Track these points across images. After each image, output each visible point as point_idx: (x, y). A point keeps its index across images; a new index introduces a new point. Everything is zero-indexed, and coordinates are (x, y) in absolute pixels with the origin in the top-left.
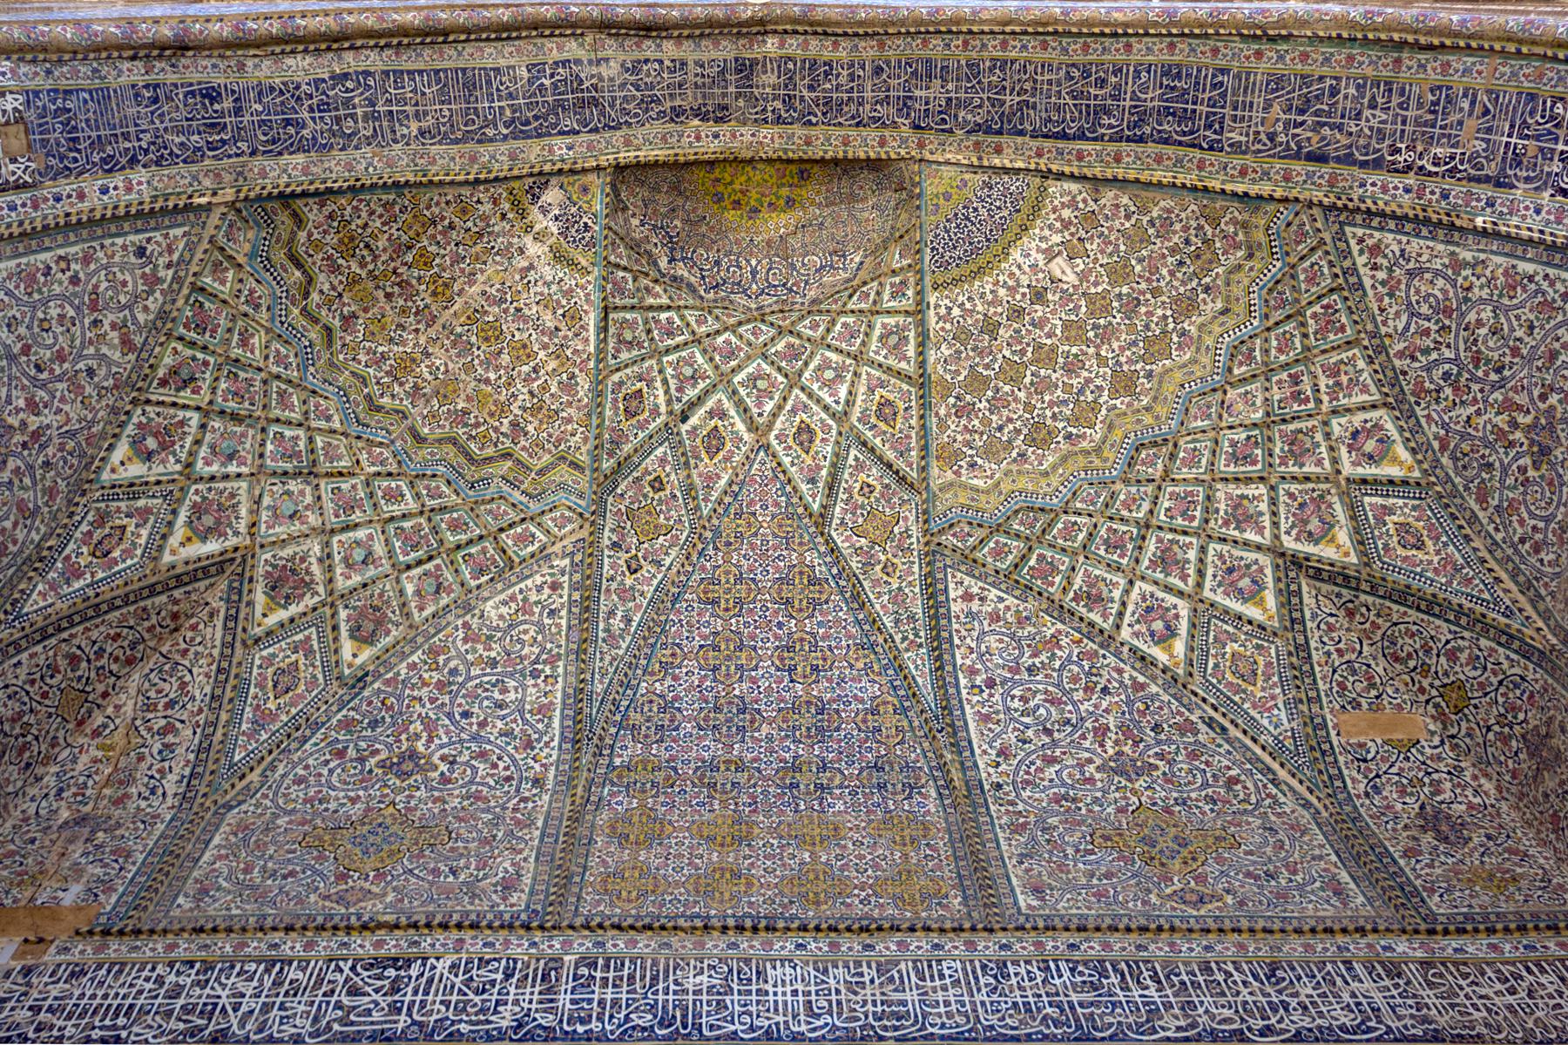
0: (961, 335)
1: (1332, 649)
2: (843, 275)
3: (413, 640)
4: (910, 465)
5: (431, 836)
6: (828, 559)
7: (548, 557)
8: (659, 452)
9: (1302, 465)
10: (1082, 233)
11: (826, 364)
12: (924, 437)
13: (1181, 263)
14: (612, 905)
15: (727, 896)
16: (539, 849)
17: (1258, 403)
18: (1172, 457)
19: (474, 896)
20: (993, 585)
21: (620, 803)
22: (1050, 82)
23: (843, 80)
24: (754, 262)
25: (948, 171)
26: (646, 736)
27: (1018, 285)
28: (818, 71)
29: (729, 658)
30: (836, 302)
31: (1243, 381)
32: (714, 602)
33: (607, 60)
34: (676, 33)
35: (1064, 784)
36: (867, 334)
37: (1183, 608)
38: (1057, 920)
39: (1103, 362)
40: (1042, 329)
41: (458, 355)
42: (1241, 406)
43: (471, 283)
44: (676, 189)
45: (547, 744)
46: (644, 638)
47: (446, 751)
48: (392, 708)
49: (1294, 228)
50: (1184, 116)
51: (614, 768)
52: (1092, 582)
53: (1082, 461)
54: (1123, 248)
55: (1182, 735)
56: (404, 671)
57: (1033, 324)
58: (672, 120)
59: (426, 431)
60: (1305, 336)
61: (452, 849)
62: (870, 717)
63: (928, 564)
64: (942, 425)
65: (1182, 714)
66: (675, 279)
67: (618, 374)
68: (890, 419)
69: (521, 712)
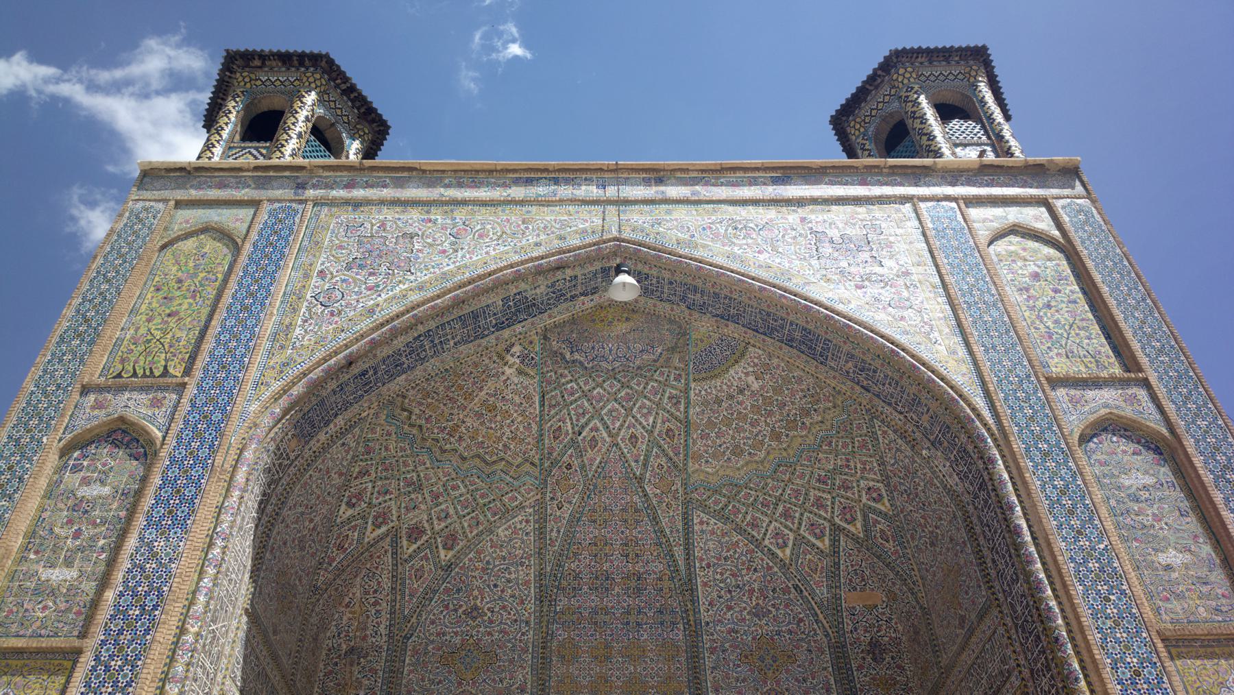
0: (705, 403)
2: (652, 357)
32: (595, 521)
39: (767, 424)
52: (754, 518)
53: (755, 466)
64: (694, 443)
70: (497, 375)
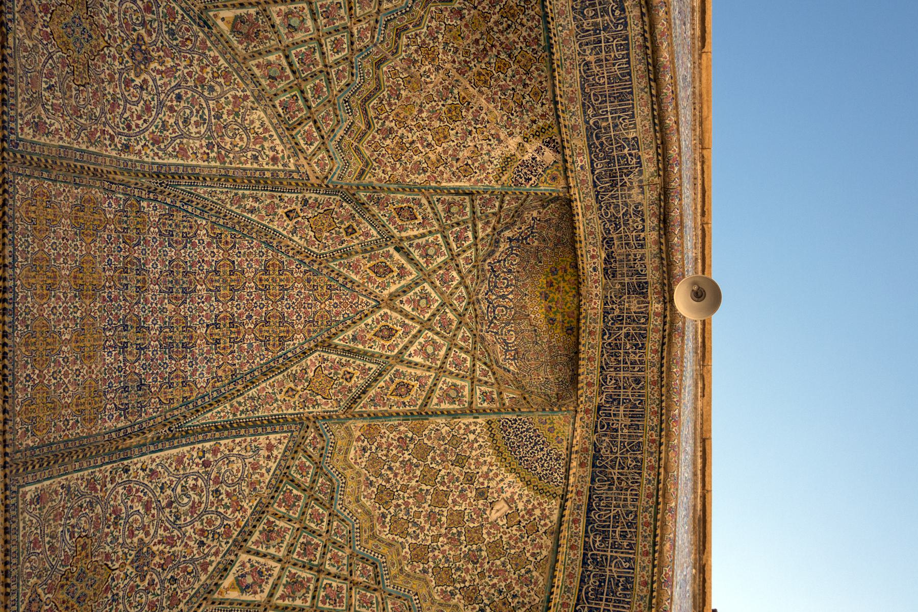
0: (455, 441)
3: (235, 60)
4: (364, 406)
5: (82, 72)
6: (298, 350)
7: (296, 154)
8: (373, 232)
11: (437, 347)
12: (384, 416)
13: (500, 592)
14: (24, 200)
15: (32, 281)
16: (71, 148)
18: (367, 588)
19: (30, 102)
20: (279, 465)
21: (110, 205)
22: (626, 500)
23: (632, 357)
24: (511, 296)
25: (570, 430)
26: (164, 224)
27: (489, 480)
28: (639, 339)
29: (225, 281)
30: (482, 354)
32: (266, 271)
33: (643, 193)
34: (663, 241)
35: (128, 516)
36: (457, 375)
37: (260, 597)
38: (13, 513)
39: (435, 539)
40: (459, 496)
41: (438, 91)
43: (488, 100)
44: (559, 242)
45: (157, 154)
46: (239, 222)
47: (151, 83)
48: (184, 45)
50: (598, 593)
51: (138, 202)
52: (281, 533)
53: (366, 525)
54: (513, 551)
55: (168, 598)
56: (212, 54)
57: (463, 490)
58: (605, 239)
59: (385, 69)
61: (69, 87)
62: (181, 380)
63: (293, 420)
64: (393, 428)
65: (184, 597)
66: (497, 242)
67: (426, 203)
68: (397, 392)
69: (181, 136)
70: (509, 124)
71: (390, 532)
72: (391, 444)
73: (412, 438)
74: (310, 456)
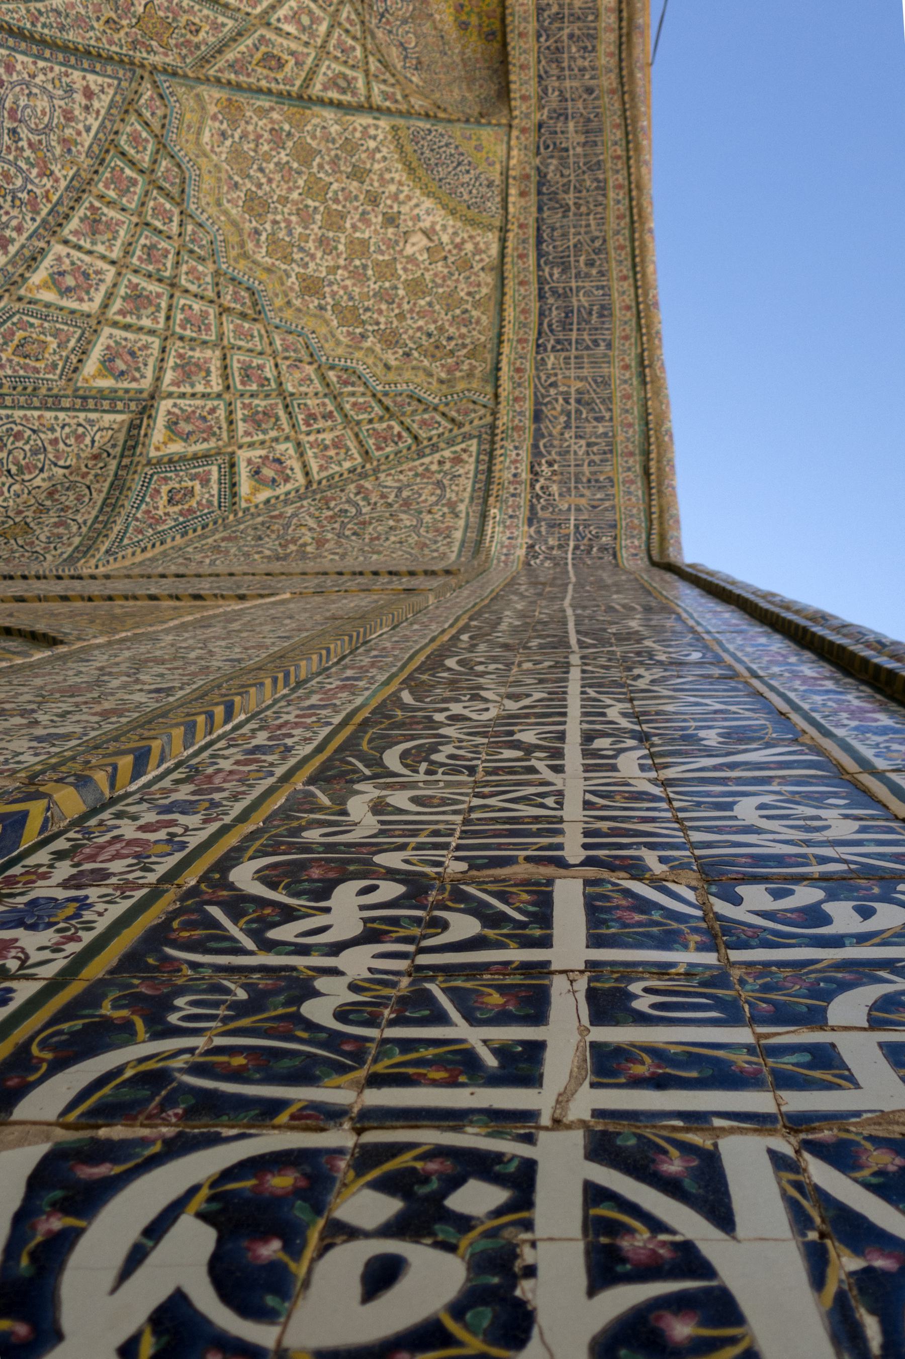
0: (349, 146)
1: (57, 434)
4: (220, 70)
9: (244, 421)
10: (451, 259)
11: (315, 20)
13: (429, 335)
17: (303, 389)
18: (243, 316)
20: (102, 126)
22: (588, 225)
27: (400, 203)
28: (587, 41)
31: (323, 377)
39: (332, 270)
42: (298, 375)
49: (471, 406)
57: (364, 213)
60: (371, 421)
64: (262, 112)
71: (268, 254)
72: (261, 136)
73: (289, 134)
74: (147, 124)
